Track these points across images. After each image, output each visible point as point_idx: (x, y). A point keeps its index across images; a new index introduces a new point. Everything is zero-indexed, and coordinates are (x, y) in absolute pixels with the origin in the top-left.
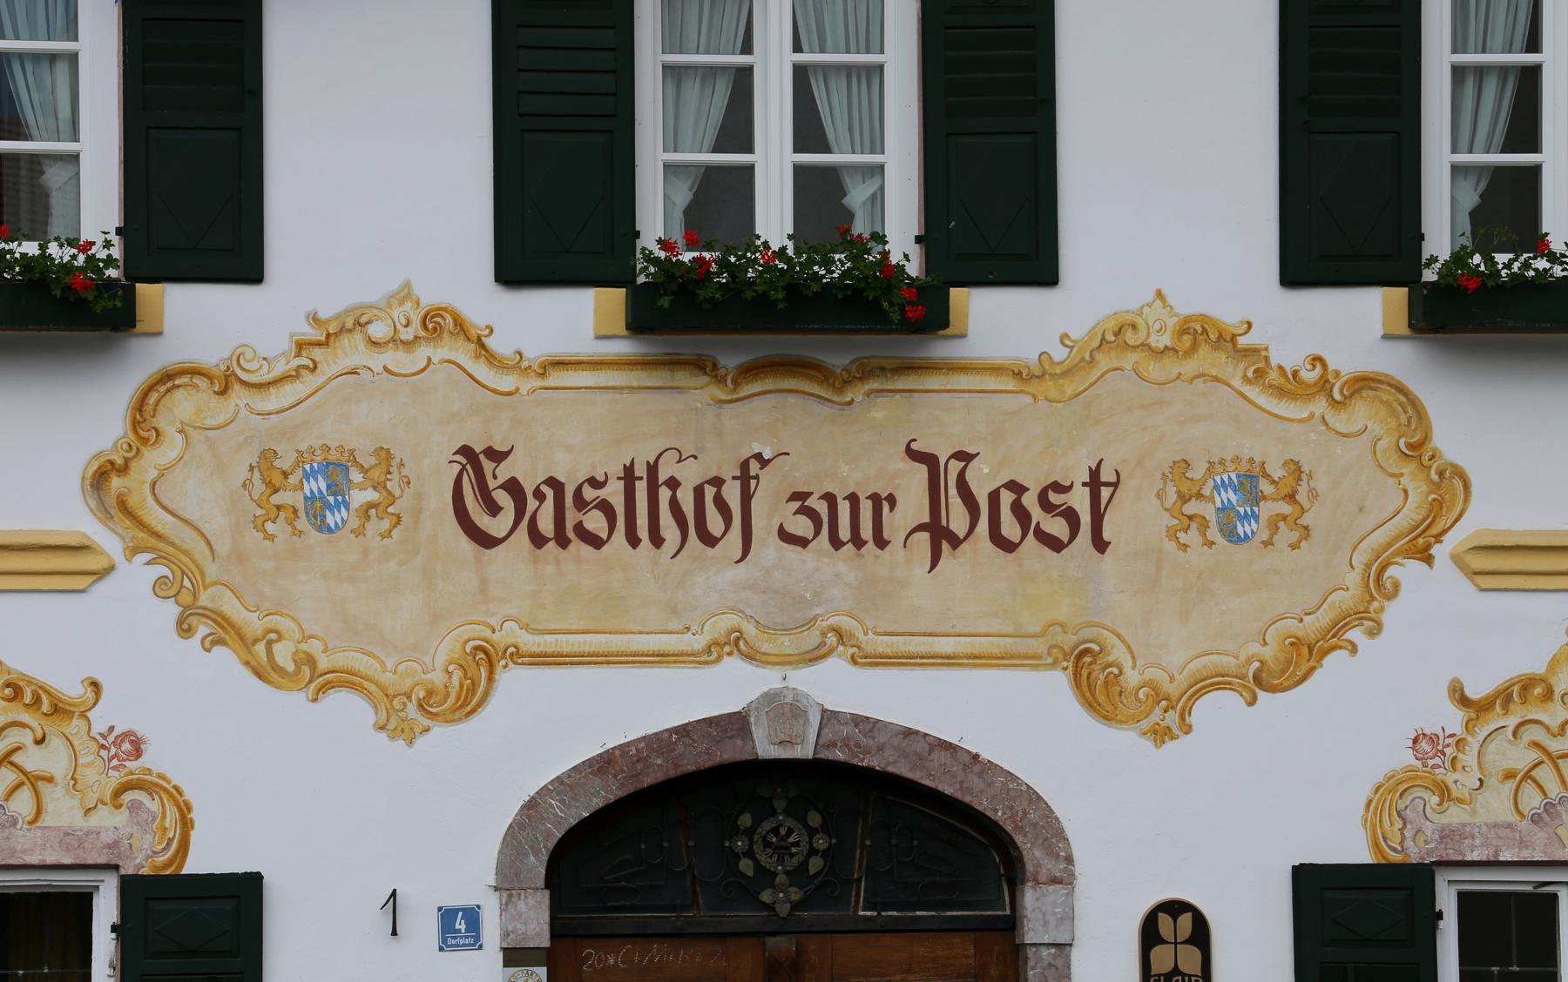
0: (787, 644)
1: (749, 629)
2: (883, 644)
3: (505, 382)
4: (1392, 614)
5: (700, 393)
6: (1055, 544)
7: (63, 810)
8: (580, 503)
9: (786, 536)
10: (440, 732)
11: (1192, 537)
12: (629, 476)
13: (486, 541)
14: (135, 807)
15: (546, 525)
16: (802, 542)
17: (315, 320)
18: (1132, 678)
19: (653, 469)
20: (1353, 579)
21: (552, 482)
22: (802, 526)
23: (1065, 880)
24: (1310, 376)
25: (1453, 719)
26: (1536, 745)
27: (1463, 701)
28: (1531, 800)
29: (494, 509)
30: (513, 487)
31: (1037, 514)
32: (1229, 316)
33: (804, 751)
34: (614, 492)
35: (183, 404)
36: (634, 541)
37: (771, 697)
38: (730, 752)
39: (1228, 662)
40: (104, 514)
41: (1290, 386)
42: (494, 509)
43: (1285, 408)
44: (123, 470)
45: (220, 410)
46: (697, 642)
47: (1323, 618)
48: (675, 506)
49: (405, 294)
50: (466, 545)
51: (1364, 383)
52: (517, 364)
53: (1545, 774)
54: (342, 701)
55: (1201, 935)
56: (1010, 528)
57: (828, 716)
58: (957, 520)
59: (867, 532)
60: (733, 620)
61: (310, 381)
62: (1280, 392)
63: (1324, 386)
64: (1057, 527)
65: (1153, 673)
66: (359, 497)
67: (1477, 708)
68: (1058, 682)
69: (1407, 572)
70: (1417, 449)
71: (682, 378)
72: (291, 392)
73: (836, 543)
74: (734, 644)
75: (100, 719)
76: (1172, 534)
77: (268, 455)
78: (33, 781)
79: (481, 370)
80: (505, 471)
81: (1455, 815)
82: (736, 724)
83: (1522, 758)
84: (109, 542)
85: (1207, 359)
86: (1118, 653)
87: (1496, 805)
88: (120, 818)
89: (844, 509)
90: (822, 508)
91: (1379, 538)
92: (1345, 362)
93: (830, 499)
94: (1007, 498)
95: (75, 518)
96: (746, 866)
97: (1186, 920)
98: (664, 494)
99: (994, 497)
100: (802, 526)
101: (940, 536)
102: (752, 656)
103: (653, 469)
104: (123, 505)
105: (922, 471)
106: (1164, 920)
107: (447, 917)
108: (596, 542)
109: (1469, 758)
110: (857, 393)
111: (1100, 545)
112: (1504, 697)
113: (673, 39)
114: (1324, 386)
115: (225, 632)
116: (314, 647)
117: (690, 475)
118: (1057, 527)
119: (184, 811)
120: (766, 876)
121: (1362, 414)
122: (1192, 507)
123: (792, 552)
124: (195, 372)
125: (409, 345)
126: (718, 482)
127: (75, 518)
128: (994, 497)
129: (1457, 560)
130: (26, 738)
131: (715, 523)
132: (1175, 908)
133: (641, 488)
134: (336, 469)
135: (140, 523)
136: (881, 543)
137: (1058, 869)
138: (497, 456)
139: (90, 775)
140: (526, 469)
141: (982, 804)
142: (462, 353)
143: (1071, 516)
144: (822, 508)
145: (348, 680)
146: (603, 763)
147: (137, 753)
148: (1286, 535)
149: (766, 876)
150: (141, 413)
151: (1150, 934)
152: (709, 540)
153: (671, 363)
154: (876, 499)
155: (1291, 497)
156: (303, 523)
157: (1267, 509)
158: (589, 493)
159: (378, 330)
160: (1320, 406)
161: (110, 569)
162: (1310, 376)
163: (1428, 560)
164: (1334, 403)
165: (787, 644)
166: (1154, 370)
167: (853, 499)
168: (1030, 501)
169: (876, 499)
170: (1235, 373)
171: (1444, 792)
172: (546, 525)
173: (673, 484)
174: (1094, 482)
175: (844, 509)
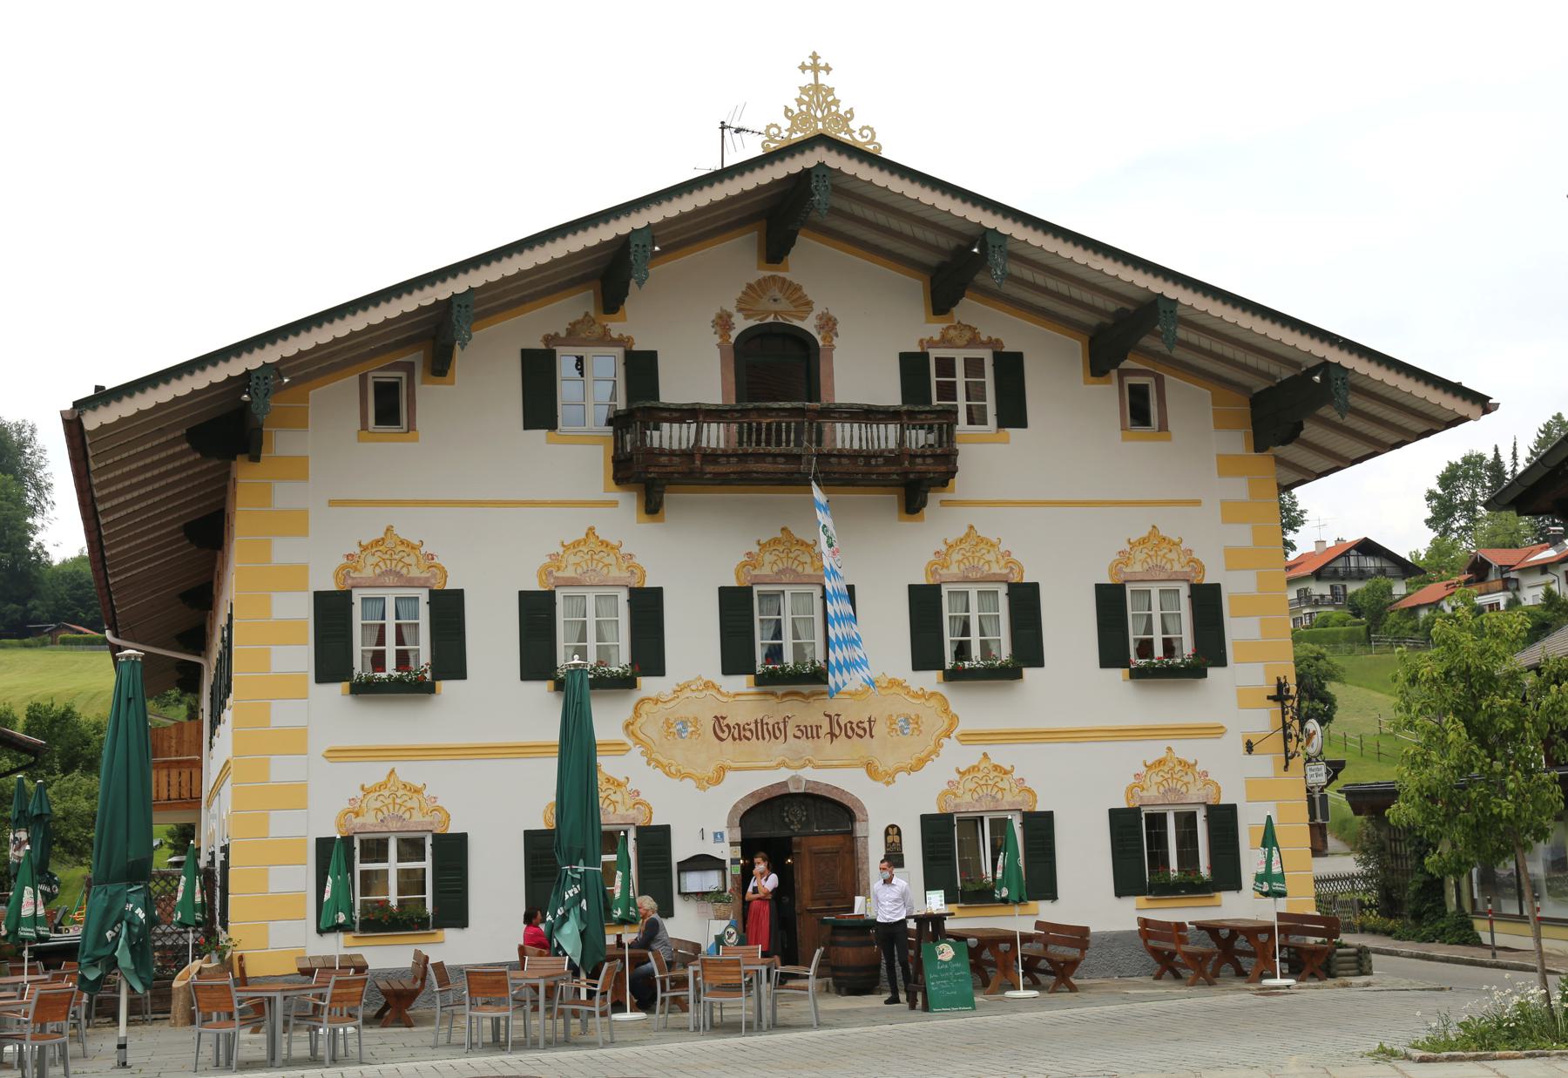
0: (797, 764)
1: (787, 761)
2: (820, 763)
3: (725, 699)
4: (942, 751)
5: (773, 701)
6: (861, 737)
7: (621, 810)
8: (744, 729)
9: (795, 736)
10: (712, 788)
11: (893, 734)
12: (756, 722)
13: (721, 740)
14: (638, 809)
15: (736, 735)
16: (799, 738)
17: (678, 685)
18: (881, 769)
19: (762, 720)
20: (932, 743)
21: (737, 724)
22: (799, 734)
23: (866, 820)
24: (920, 693)
25: (956, 777)
27: (959, 772)
28: (976, 796)
29: (723, 732)
30: (728, 726)
31: (856, 729)
32: (901, 679)
33: (802, 791)
34: (753, 726)
35: (647, 707)
36: (758, 739)
37: (793, 777)
39: (903, 765)
40: (628, 736)
41: (916, 696)
42: (723, 732)
43: (914, 701)
44: (632, 724)
45: (655, 709)
47: (925, 753)
48: (768, 729)
49: (700, 678)
50: (717, 741)
51: (933, 694)
52: (727, 695)
53: (979, 790)
54: (688, 781)
55: (899, 833)
56: (850, 733)
57: (807, 781)
58: (837, 731)
59: (815, 735)
60: (783, 758)
61: (678, 700)
63: (924, 695)
64: (861, 732)
65: (885, 768)
66: (690, 729)
68: (863, 771)
69: (945, 741)
70: (946, 710)
71: (768, 697)
72: (672, 703)
73: (807, 738)
74: (783, 764)
75: (629, 787)
76: (889, 733)
77: (667, 719)
78: (614, 803)
79: (719, 697)
80: (725, 722)
81: (958, 801)
82: (785, 784)
83: (973, 786)
84: (630, 743)
85: (896, 689)
86: (877, 764)
87: (968, 798)
88: (635, 811)
89: (809, 729)
90: (804, 729)
91: (937, 733)
92: (928, 690)
93: (806, 727)
94: (849, 725)
95: (622, 737)
96: (787, 820)
97: (895, 829)
98: (765, 727)
99: (846, 725)
100: (799, 734)
101: (833, 735)
102: (788, 767)
103: (762, 720)
104: (632, 733)
105: (828, 719)
106: (890, 829)
107: (715, 834)
108: (749, 739)
109: (961, 786)
110: (811, 700)
111: (872, 736)
112: (968, 771)
113: (761, 613)
114: (924, 695)
115: (659, 764)
116: (680, 767)
117: (771, 722)
118: (861, 732)
119: (650, 809)
120: (792, 823)
121: (933, 702)
122: (893, 726)
123: (797, 740)
124: (650, 699)
125: (701, 691)
126: (778, 723)
127: (622, 737)
128: (846, 725)
129: (956, 737)
130: (611, 792)
131: (778, 734)
132: (893, 826)
133: (759, 725)
134: (684, 723)
135: (637, 737)
136: (818, 737)
137: (864, 818)
138: (724, 718)
139: (627, 801)
140: (731, 721)
141: (845, 802)
142: (714, 692)
143: (864, 729)
144: (804, 729)
145: (689, 776)
146: (752, 795)
147: (638, 795)
148: (916, 732)
149: (792, 823)
150: (636, 709)
151: (887, 833)
152: (777, 738)
153: (765, 693)
155: (917, 723)
156: (676, 736)
157: (911, 726)
158: (747, 727)
159: (693, 687)
160: (923, 700)
162: (920, 693)
165: (797, 764)
166: (883, 692)
168: (854, 726)
170: (902, 692)
171: (955, 795)
172: (736, 735)
173: (767, 724)
174: (870, 721)
175: (809, 729)
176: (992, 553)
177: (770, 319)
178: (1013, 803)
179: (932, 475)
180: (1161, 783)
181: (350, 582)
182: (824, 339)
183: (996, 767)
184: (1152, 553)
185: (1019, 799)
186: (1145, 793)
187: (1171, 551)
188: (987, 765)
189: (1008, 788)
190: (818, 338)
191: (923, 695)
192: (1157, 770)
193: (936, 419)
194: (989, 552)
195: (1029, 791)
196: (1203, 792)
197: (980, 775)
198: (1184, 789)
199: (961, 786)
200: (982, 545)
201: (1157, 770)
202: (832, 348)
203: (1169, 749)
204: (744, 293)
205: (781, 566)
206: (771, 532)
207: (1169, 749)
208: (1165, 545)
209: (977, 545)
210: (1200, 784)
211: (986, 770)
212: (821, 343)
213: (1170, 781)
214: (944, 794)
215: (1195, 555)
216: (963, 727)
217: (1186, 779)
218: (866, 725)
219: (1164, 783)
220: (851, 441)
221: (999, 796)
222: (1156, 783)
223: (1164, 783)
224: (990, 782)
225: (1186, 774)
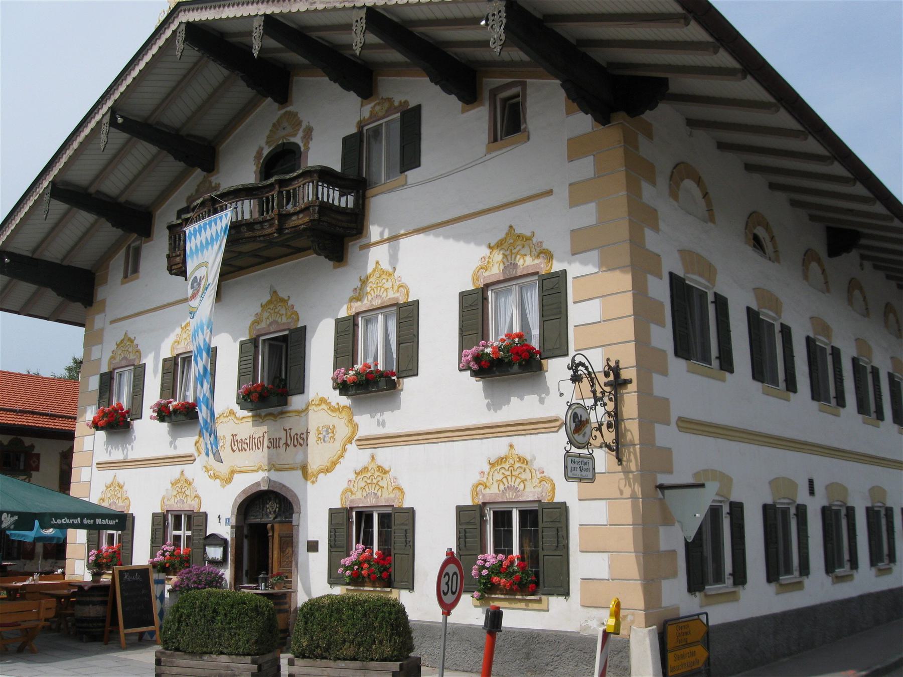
24: (337, 407)
26: (366, 482)
29: (235, 445)
30: (237, 441)
31: (299, 440)
34: (248, 441)
38: (258, 489)
46: (256, 468)
58: (289, 442)
59: (278, 445)
62: (332, 411)
63: (338, 409)
67: (357, 474)
69: (349, 446)
73: (274, 447)
81: (353, 497)
82: (258, 484)
85: (324, 406)
93: (273, 439)
101: (287, 444)
108: (245, 450)
125: (227, 416)
136: (279, 447)
138: (236, 435)
148: (332, 440)
152: (258, 449)
154: (279, 438)
155: (333, 432)
158: (245, 441)
161: (195, 460)
162: (337, 407)
163: (351, 443)
164: (340, 412)
167: (276, 439)
169: (279, 438)
171: (351, 492)
173: (255, 438)
176: (390, 281)
177: (280, 142)
178: (387, 500)
179: (302, 227)
180: (501, 481)
181: (112, 366)
182: (305, 145)
183: (380, 468)
184: (508, 253)
185: (392, 496)
186: (487, 491)
187: (523, 247)
188: (374, 466)
189: (385, 486)
190: (301, 145)
191: (338, 409)
192: (499, 468)
193: (303, 180)
194: (387, 280)
195: (400, 489)
196: (538, 490)
197: (368, 475)
198: (521, 487)
199: (355, 485)
200: (384, 276)
201: (499, 468)
202: (308, 149)
203: (511, 446)
204: (270, 131)
205: (271, 320)
206: (266, 298)
207: (511, 446)
208: (519, 242)
209: (380, 275)
210: (535, 481)
211: (372, 471)
212: (302, 149)
213: (509, 478)
214: (347, 490)
215: (545, 246)
216: (361, 433)
217: (523, 476)
218: (304, 436)
219: (505, 480)
220: (243, 213)
221: (379, 494)
222: (498, 481)
223: (505, 480)
224: (375, 481)
225: (525, 471)
